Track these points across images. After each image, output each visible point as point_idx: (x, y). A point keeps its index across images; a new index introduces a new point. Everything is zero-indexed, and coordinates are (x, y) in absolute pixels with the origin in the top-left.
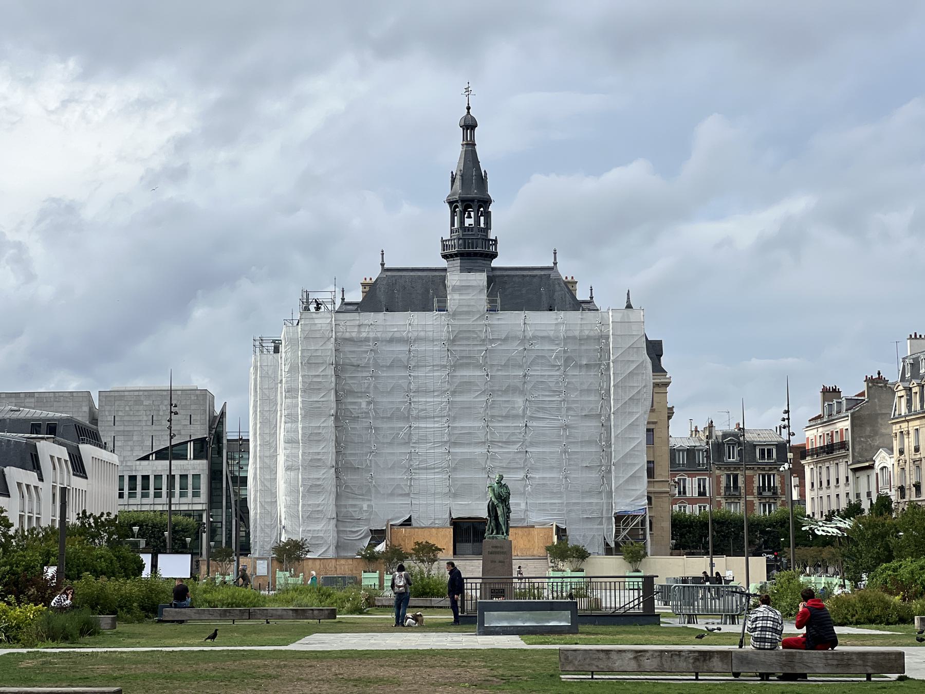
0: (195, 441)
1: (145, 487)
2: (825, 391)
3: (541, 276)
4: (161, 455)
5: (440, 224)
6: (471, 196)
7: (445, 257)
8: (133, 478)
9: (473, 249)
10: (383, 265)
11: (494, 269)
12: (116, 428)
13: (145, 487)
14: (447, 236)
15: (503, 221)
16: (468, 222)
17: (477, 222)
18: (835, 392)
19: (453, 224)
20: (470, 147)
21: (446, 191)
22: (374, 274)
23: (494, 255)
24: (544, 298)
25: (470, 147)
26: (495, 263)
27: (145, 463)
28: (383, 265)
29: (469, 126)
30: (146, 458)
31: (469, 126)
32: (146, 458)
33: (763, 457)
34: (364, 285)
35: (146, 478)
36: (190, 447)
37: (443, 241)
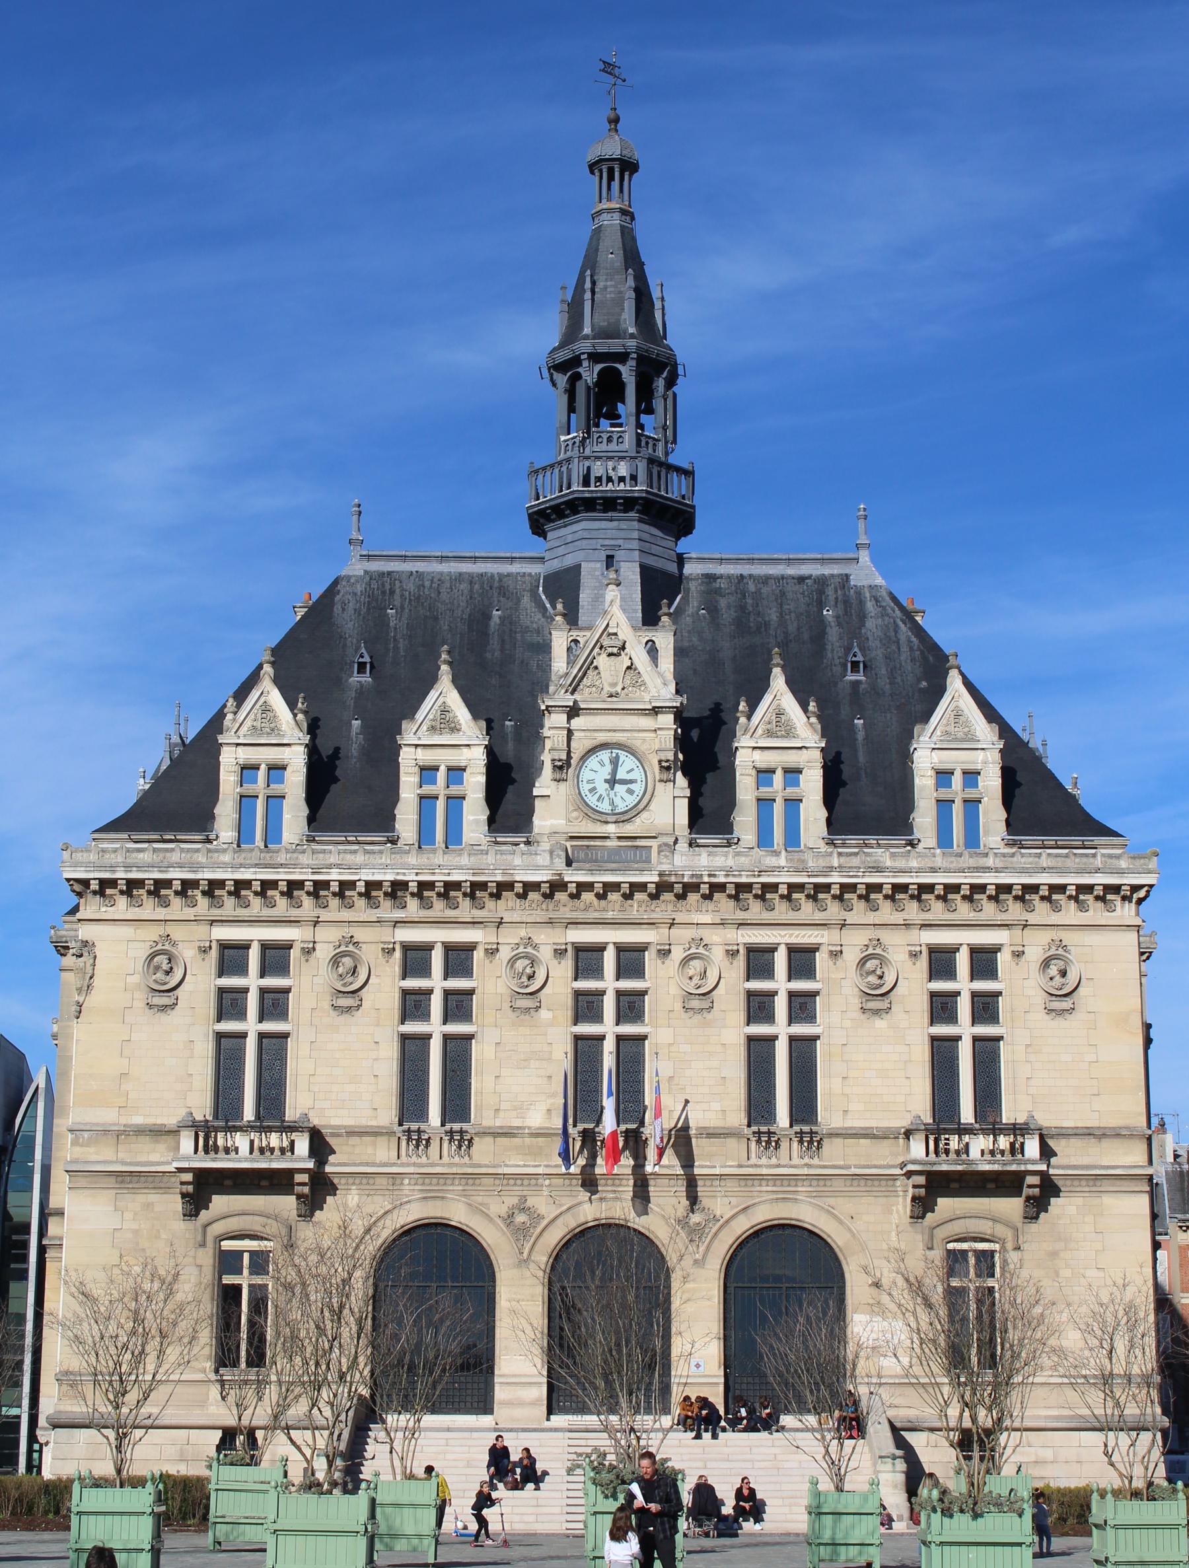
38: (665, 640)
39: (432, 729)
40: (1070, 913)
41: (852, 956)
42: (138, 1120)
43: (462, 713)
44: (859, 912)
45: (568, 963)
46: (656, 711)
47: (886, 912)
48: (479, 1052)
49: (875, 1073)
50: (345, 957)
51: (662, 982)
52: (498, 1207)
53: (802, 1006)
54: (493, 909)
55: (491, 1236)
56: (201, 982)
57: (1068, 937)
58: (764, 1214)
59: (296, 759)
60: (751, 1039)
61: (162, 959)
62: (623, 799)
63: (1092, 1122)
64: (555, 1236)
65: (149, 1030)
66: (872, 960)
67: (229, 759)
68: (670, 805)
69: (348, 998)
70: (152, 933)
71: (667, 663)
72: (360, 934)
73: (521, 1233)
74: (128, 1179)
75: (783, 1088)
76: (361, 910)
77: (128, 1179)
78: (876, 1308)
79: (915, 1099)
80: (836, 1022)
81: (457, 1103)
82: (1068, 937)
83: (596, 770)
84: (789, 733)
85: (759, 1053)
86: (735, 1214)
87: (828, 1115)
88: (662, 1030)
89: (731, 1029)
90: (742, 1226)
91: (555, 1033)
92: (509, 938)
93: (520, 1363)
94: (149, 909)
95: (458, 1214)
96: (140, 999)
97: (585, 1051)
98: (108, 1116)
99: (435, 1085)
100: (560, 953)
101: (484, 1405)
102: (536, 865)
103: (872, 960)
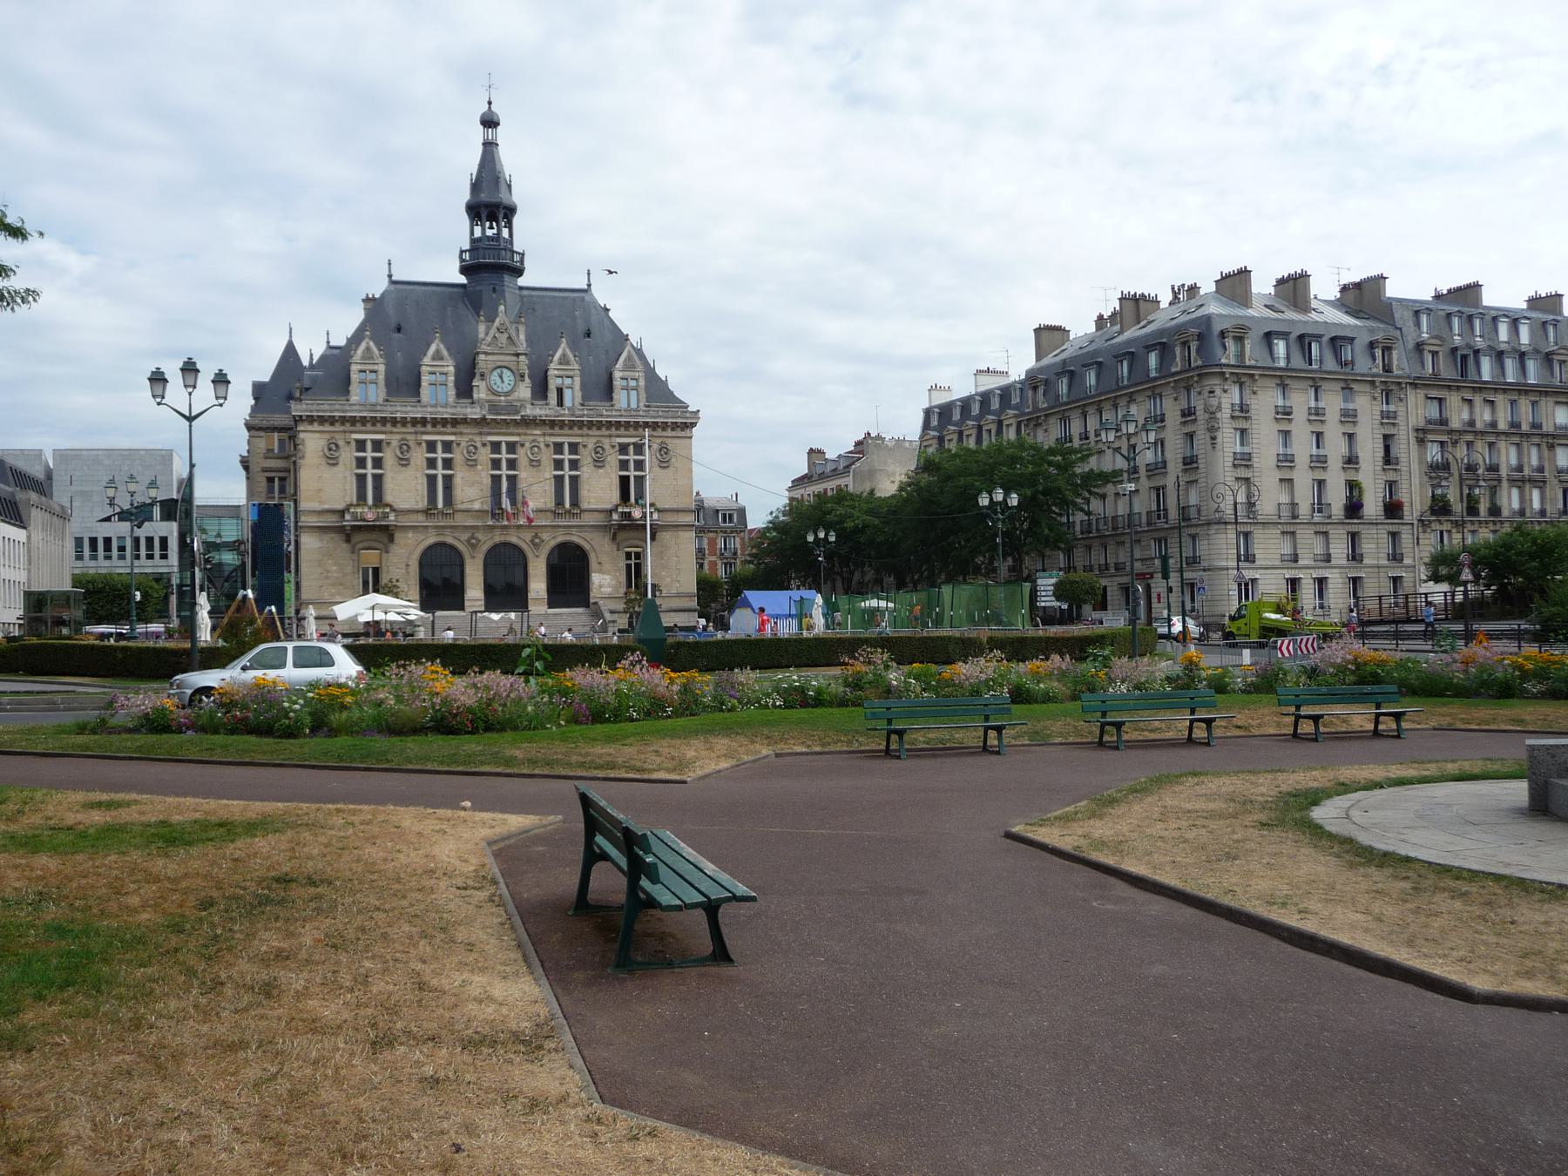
0: (162, 502)
1: (108, 548)
2: (811, 451)
3: (574, 299)
4: (123, 516)
5: (460, 232)
6: (490, 204)
7: (464, 270)
8: (93, 541)
9: (491, 265)
10: (390, 276)
11: (521, 288)
12: (73, 488)
13: (108, 548)
14: (467, 247)
15: (525, 234)
16: (489, 233)
17: (499, 230)
18: (820, 452)
19: (472, 233)
20: (489, 146)
21: (465, 195)
22: (378, 288)
23: (519, 272)
24: (579, 321)
25: (489, 146)
26: (522, 281)
27: (107, 524)
28: (390, 276)
29: (489, 122)
30: (108, 519)
31: (489, 122)
32: (108, 519)
33: (724, 520)
34: (367, 300)
35: (108, 541)
36: (157, 511)
37: (462, 252)
38: (522, 329)
39: (434, 359)
40: (669, 433)
41: (591, 446)
42: (326, 507)
43: (445, 353)
44: (594, 432)
45: (489, 448)
46: (518, 355)
47: (604, 432)
48: (458, 481)
49: (600, 490)
50: (404, 447)
51: (522, 455)
52: (465, 536)
53: (574, 465)
54: (461, 428)
55: (461, 547)
56: (348, 455)
57: (668, 441)
58: (560, 539)
59: (382, 368)
60: (556, 477)
61: (333, 447)
62: (506, 388)
63: (675, 506)
64: (485, 548)
65: (327, 473)
66: (599, 449)
67: (354, 368)
68: (525, 391)
69: (404, 462)
70: (327, 436)
71: (522, 337)
72: (409, 437)
73: (473, 546)
74: (323, 529)
75: (567, 493)
76: (410, 429)
77: (323, 529)
78: (600, 571)
79: (615, 496)
80: (586, 471)
81: (449, 499)
82: (668, 441)
83: (495, 376)
84: (568, 363)
85: (559, 480)
86: (551, 540)
87: (585, 506)
88: (524, 474)
89: (549, 472)
90: (553, 543)
91: (484, 475)
92: (463, 440)
93: (474, 592)
94: (327, 428)
95: (450, 540)
96: (323, 461)
97: (496, 480)
98: (316, 506)
99: (441, 491)
100: (484, 445)
101: (460, 606)
102: (474, 413)
103: (599, 449)
